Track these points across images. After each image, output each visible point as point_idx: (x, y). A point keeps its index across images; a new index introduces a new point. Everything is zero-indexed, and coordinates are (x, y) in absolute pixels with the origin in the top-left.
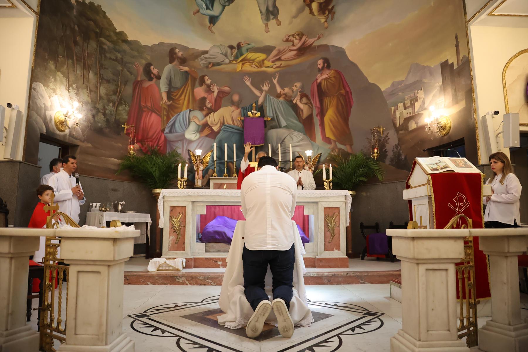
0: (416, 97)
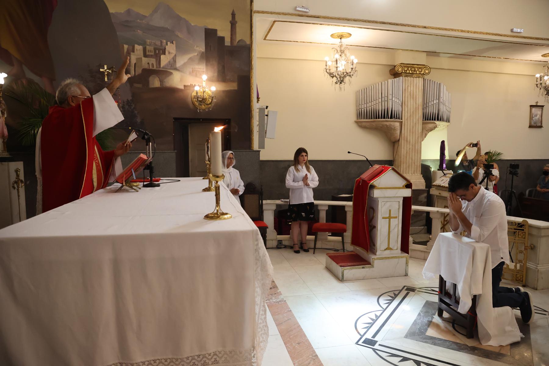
0: (164, 48)
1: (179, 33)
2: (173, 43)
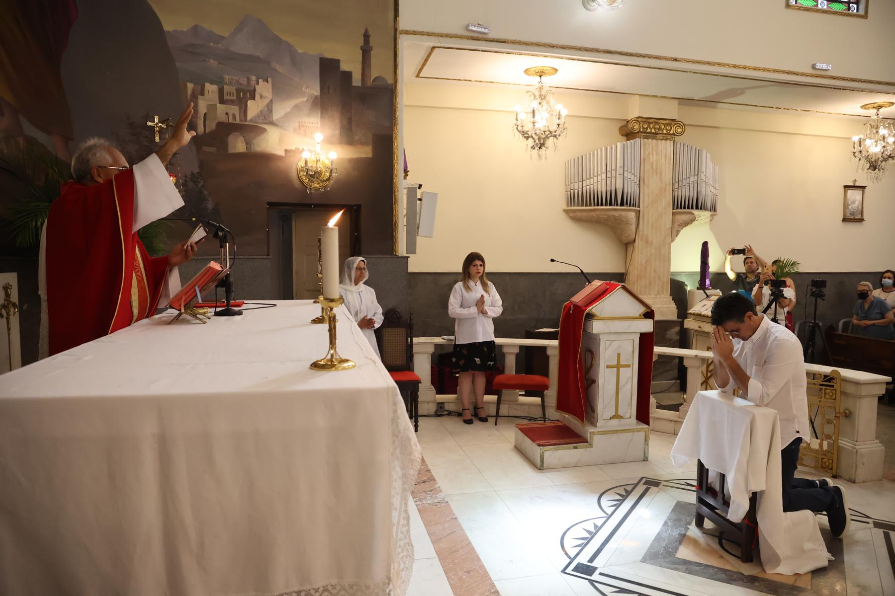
0: (253, 89)
1: (277, 65)
2: (267, 82)
